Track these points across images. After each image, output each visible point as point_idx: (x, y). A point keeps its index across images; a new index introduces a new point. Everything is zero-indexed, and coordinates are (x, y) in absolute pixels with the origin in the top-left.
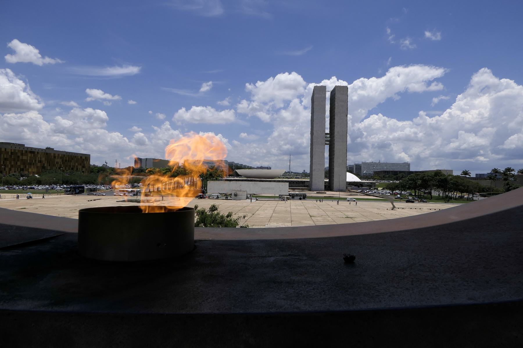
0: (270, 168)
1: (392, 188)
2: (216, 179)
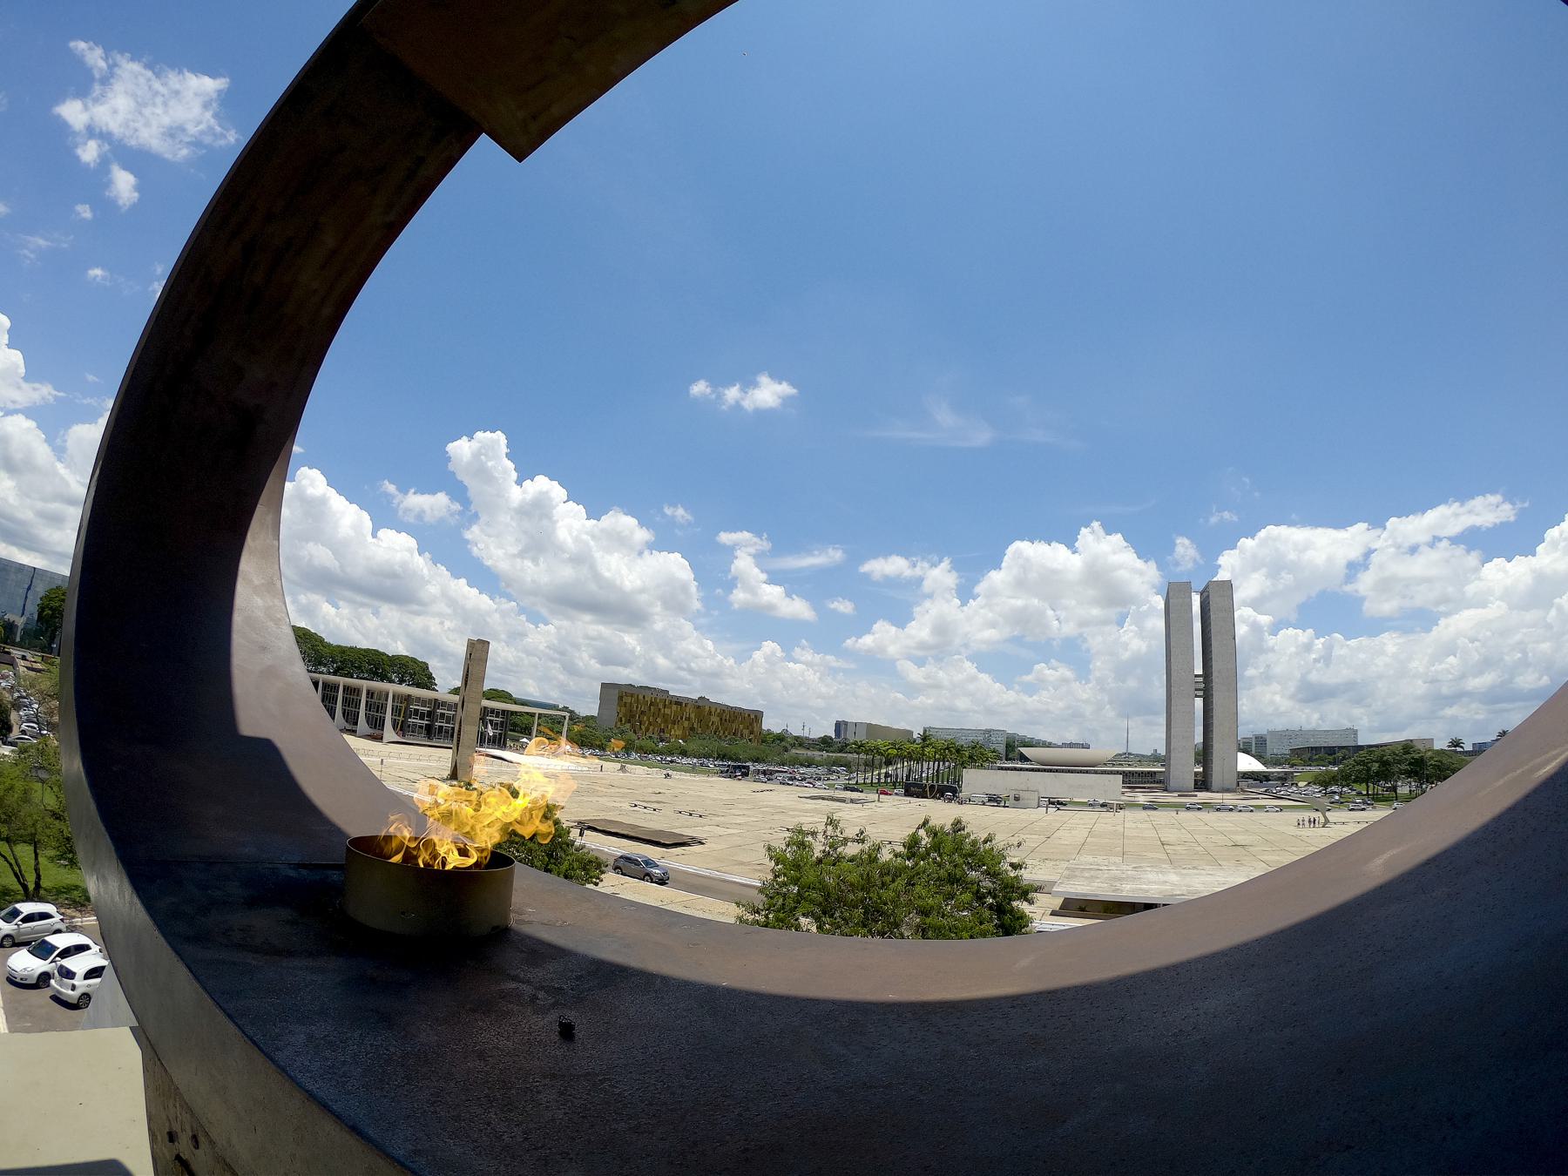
0: (1086, 746)
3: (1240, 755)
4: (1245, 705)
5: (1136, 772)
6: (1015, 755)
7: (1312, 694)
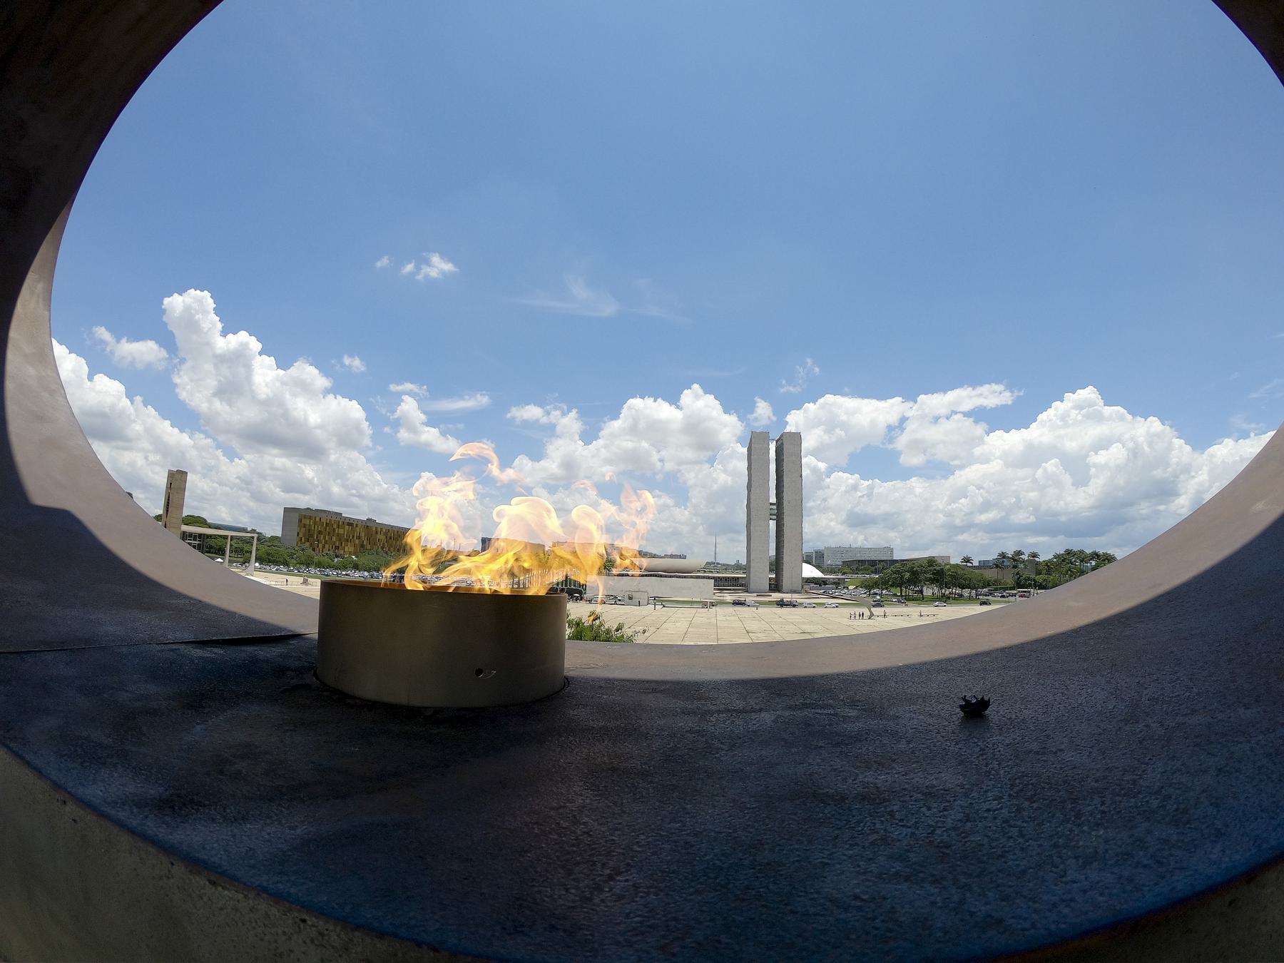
0: (685, 557)
1: (869, 586)
3: (805, 566)
4: (807, 528)
5: (724, 578)
7: (858, 521)
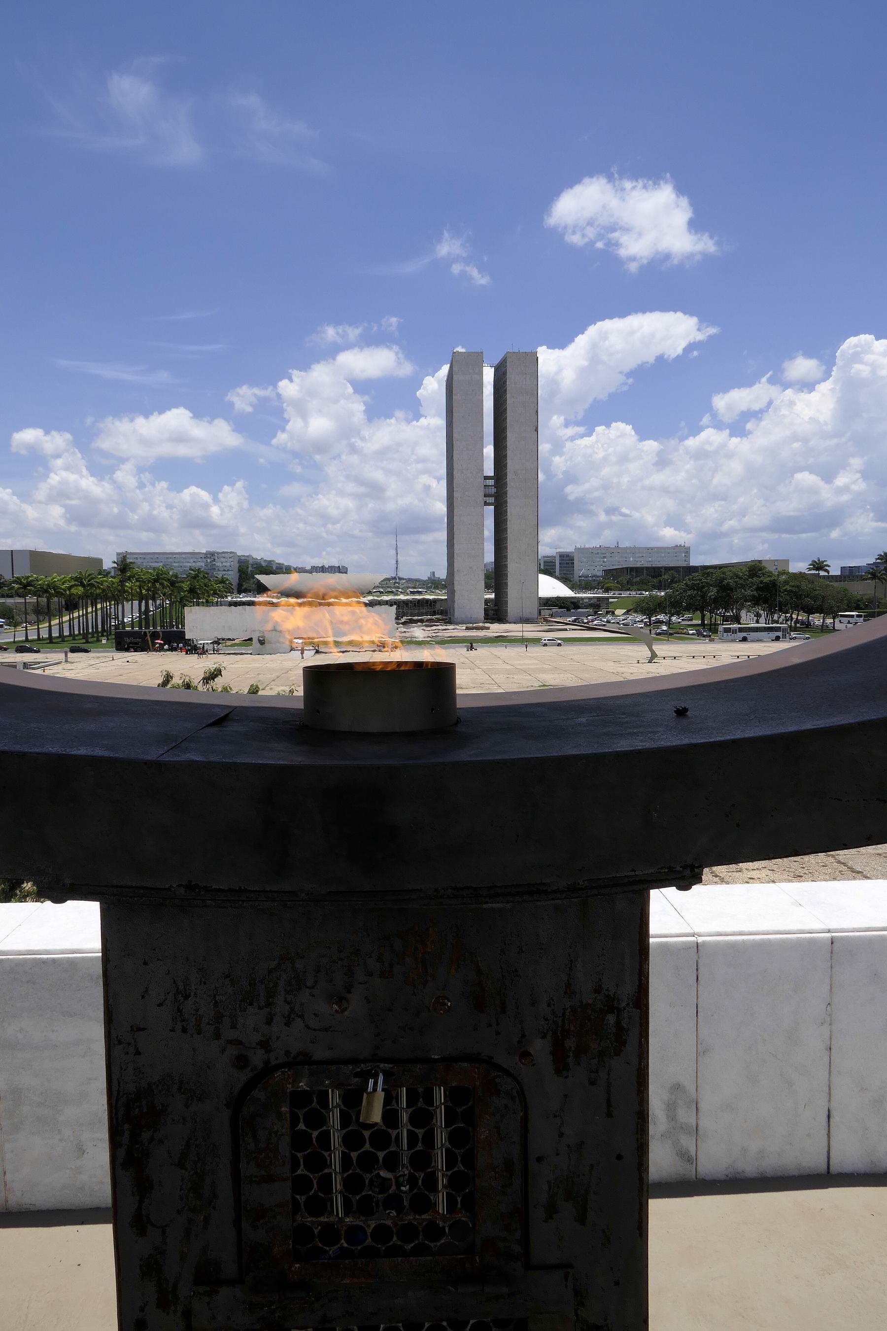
1: (648, 609)
2: (208, 603)
6: (250, 584)
